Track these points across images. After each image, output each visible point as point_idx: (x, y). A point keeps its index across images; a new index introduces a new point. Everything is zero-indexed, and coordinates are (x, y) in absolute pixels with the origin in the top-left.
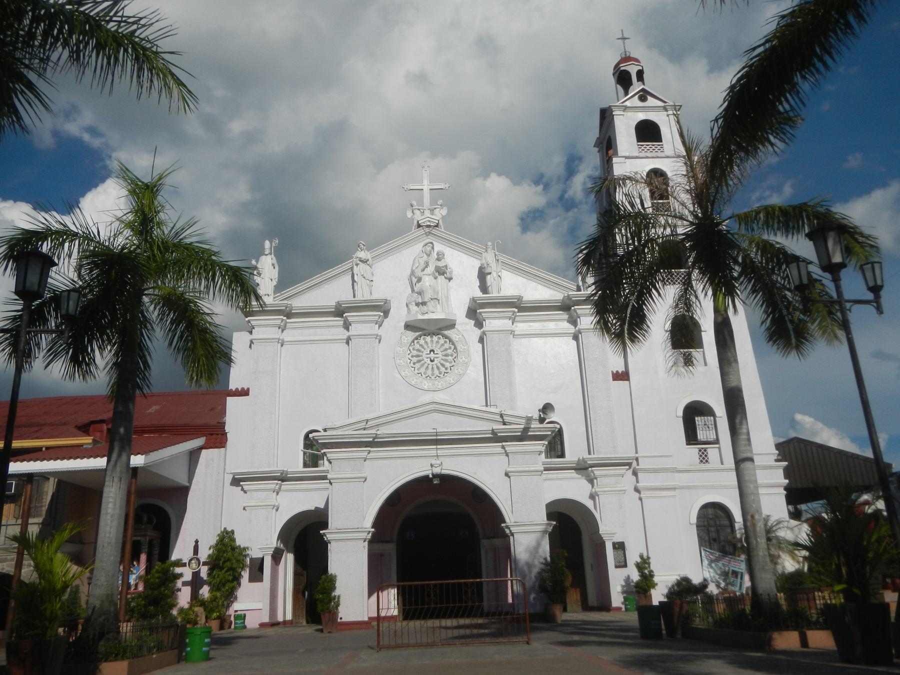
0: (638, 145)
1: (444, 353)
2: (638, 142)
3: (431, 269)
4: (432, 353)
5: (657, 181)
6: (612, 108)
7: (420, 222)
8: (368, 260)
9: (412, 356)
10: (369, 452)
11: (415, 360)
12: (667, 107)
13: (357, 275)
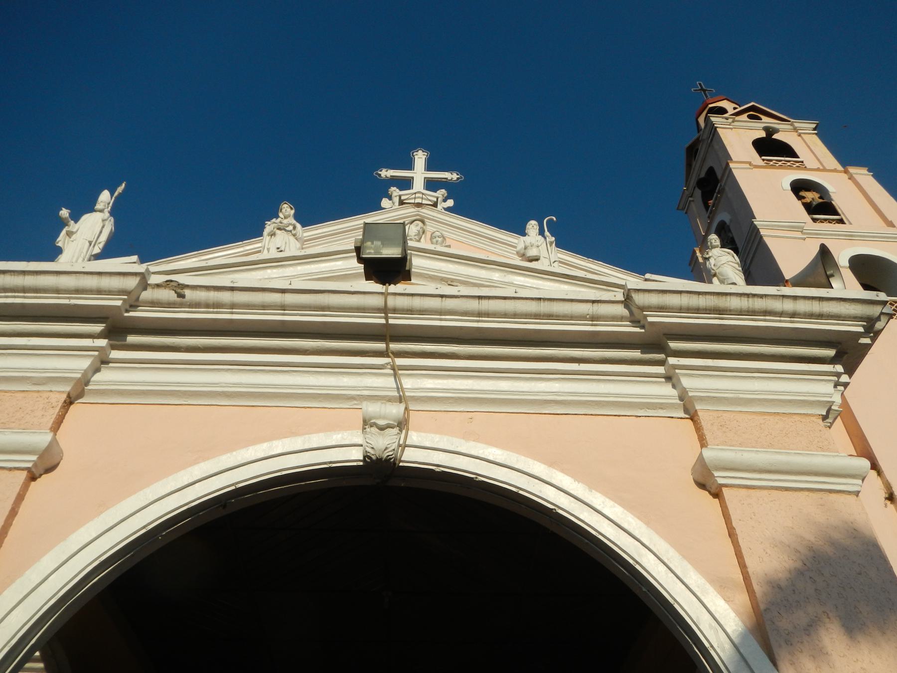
2: (761, 157)
5: (810, 196)
6: (713, 119)
7: (402, 198)
8: (295, 228)
10: (104, 361)
12: (796, 125)
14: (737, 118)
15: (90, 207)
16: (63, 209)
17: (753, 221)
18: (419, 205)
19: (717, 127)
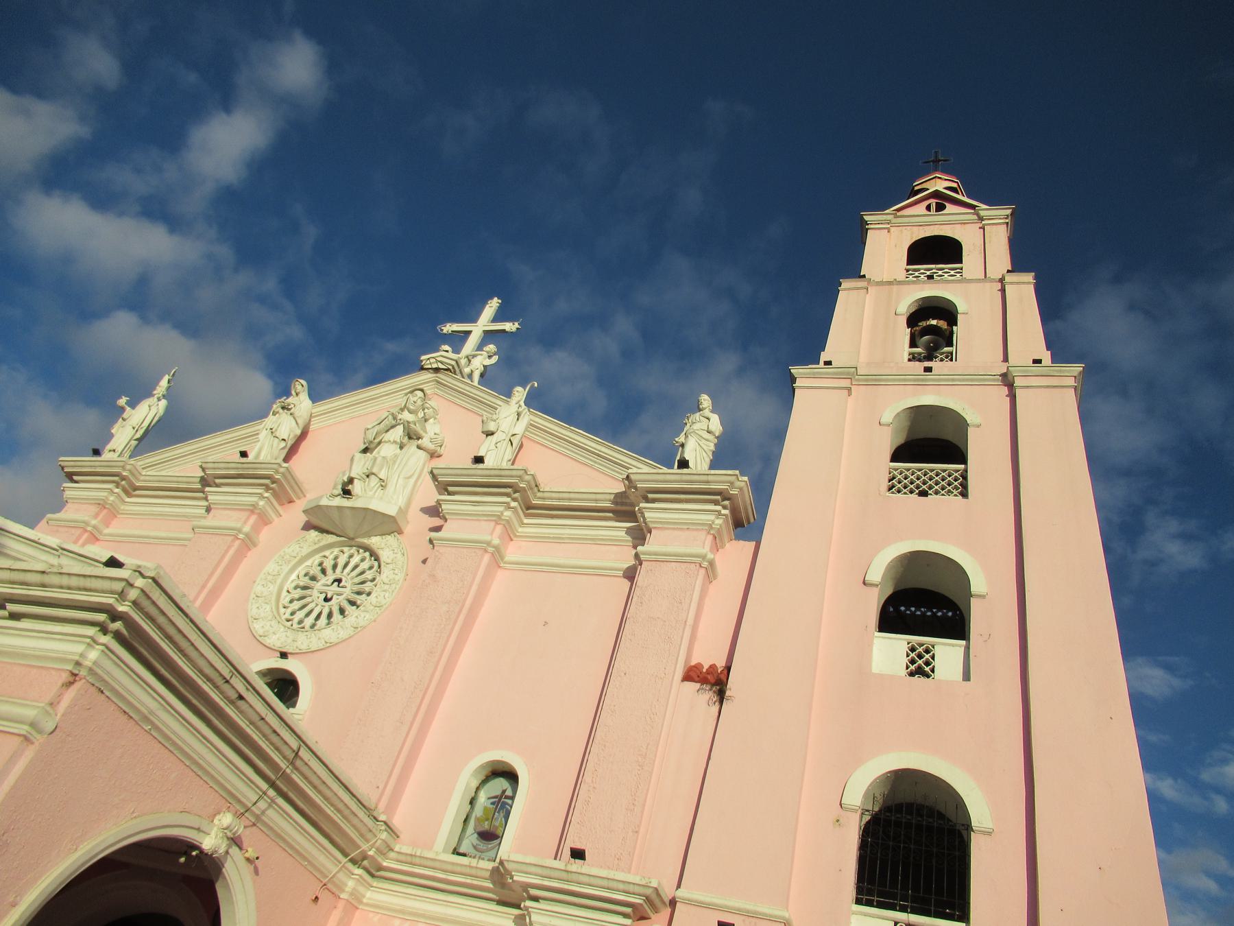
0: (908, 271)
1: (356, 588)
2: (908, 264)
3: (398, 433)
4: (336, 583)
6: (866, 218)
9: (296, 588)
11: (299, 593)
12: (982, 213)
13: (267, 429)
14: (899, 214)
15: (148, 394)
16: (123, 397)
17: (790, 369)
18: (437, 370)
19: (867, 229)
